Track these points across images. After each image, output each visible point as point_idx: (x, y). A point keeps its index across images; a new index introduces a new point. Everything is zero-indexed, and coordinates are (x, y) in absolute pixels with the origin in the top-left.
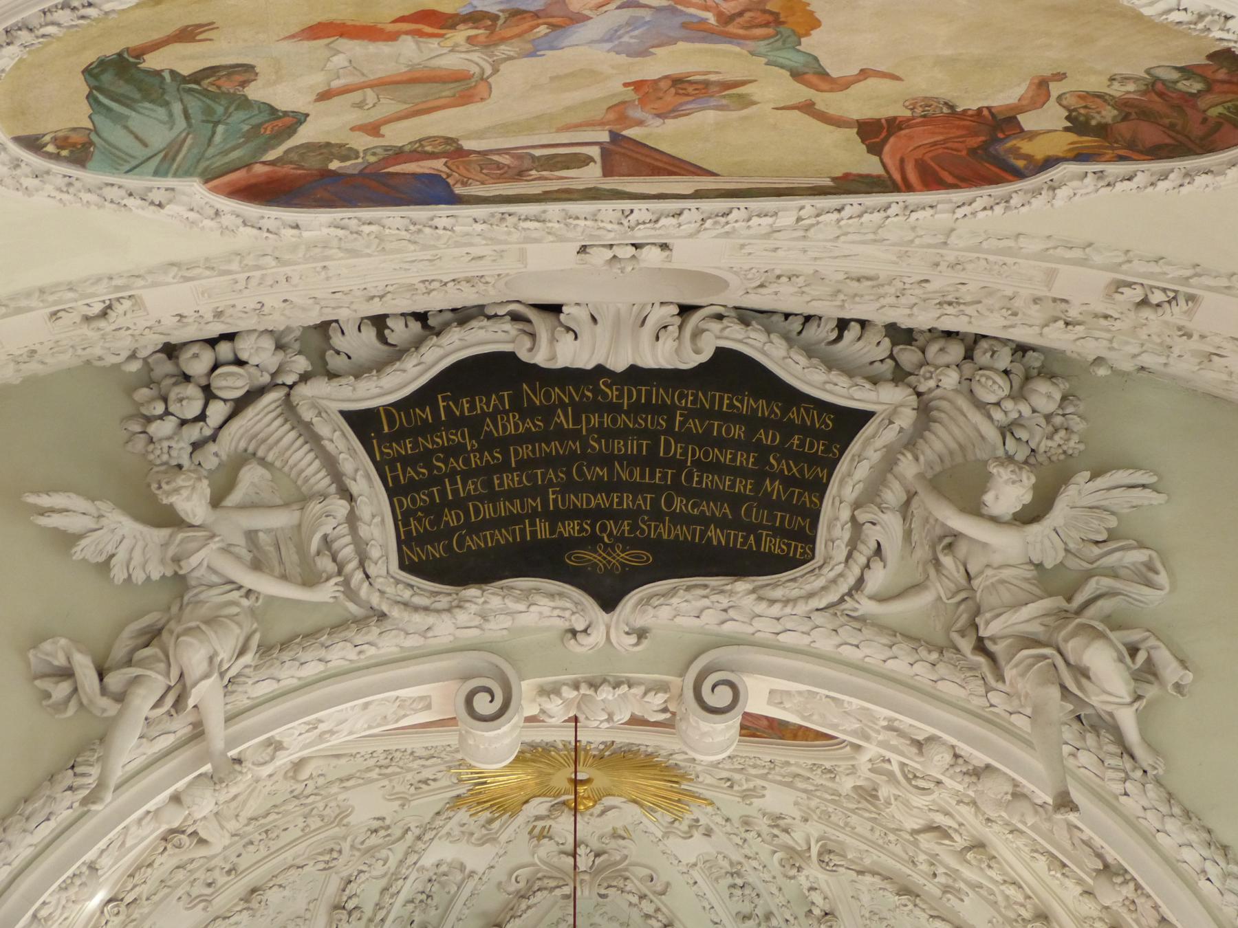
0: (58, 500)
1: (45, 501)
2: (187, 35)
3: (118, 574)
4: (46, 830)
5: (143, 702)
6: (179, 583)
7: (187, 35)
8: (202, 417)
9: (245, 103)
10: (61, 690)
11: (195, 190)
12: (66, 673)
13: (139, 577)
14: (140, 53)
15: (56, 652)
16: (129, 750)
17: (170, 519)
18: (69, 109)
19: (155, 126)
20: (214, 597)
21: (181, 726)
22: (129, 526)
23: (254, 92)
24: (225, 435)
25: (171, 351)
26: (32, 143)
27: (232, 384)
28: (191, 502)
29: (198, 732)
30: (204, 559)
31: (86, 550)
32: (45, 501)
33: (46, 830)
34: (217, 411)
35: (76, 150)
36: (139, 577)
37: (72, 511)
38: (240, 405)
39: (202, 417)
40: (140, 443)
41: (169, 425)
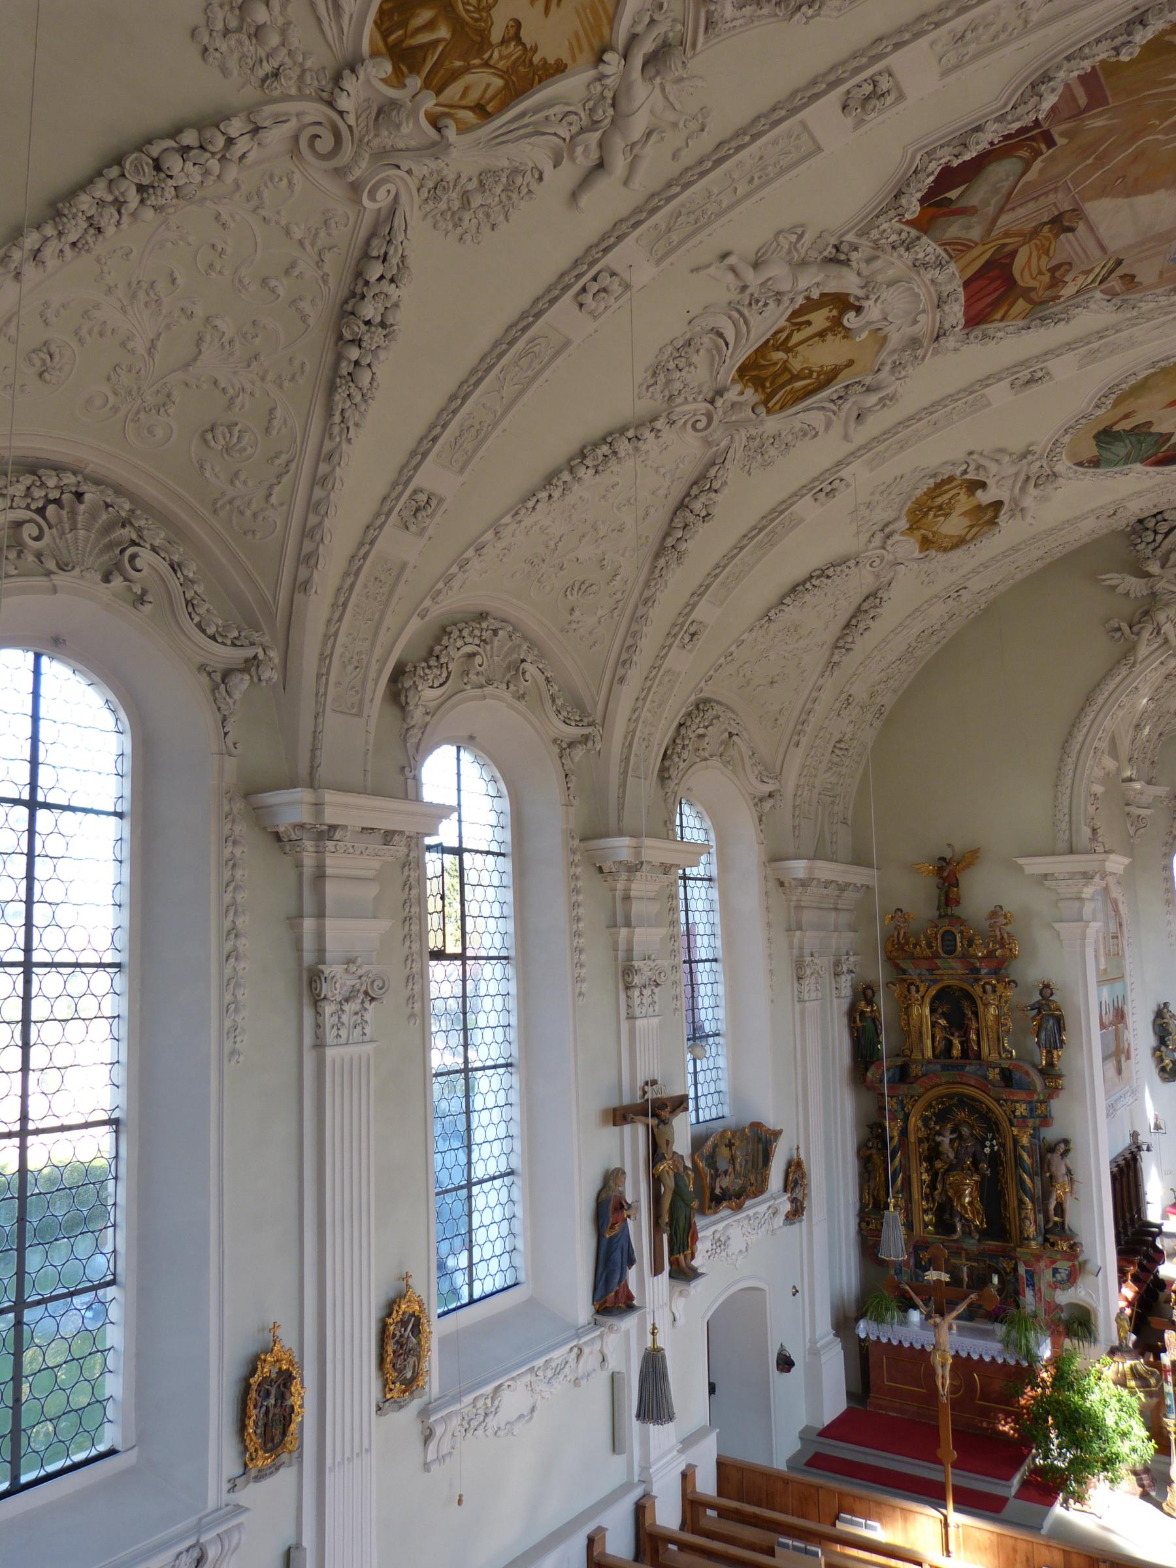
0: (1108, 576)
1: (1104, 577)
2: (1127, 416)
3: (1132, 596)
4: (1119, 679)
5: (1146, 635)
6: (1153, 595)
7: (1127, 416)
8: (1154, 541)
9: (1151, 434)
10: (1118, 635)
11: (1138, 467)
12: (1119, 629)
13: (1139, 595)
14: (1111, 426)
15: (1114, 623)
16: (1143, 650)
17: (1148, 575)
18: (1090, 450)
19: (1120, 449)
20: (1166, 597)
21: (1160, 640)
22: (1133, 580)
23: (1153, 430)
24: (1163, 545)
25: (1141, 521)
26: (1080, 464)
27: (1163, 527)
28: (1154, 568)
29: (1166, 641)
30: (1160, 586)
31: (1120, 589)
32: (1104, 577)
33: (1119, 679)
34: (1159, 538)
35: (1095, 463)
36: (1139, 595)
37: (1113, 578)
38: (1167, 534)
39: (1154, 541)
40: (1134, 553)
41: (1143, 545)
